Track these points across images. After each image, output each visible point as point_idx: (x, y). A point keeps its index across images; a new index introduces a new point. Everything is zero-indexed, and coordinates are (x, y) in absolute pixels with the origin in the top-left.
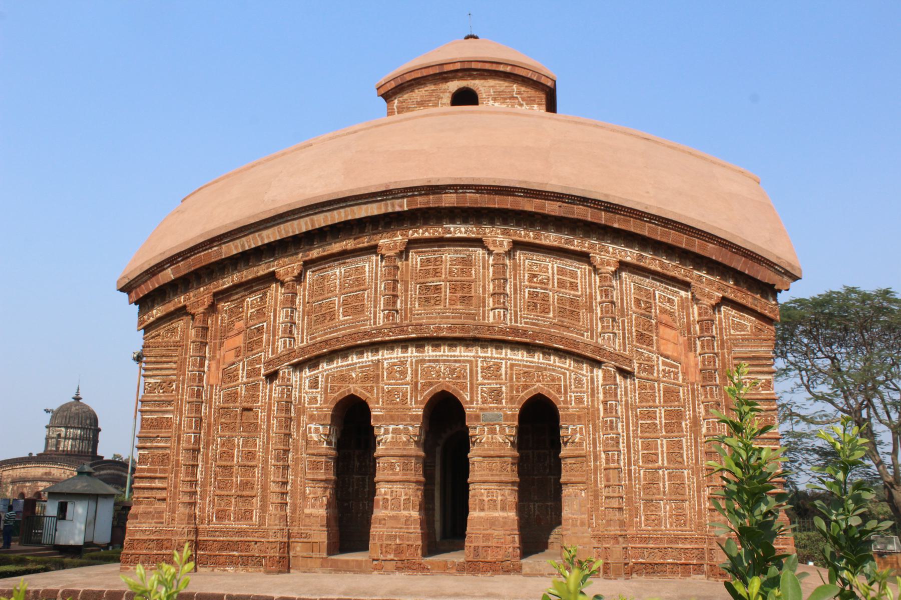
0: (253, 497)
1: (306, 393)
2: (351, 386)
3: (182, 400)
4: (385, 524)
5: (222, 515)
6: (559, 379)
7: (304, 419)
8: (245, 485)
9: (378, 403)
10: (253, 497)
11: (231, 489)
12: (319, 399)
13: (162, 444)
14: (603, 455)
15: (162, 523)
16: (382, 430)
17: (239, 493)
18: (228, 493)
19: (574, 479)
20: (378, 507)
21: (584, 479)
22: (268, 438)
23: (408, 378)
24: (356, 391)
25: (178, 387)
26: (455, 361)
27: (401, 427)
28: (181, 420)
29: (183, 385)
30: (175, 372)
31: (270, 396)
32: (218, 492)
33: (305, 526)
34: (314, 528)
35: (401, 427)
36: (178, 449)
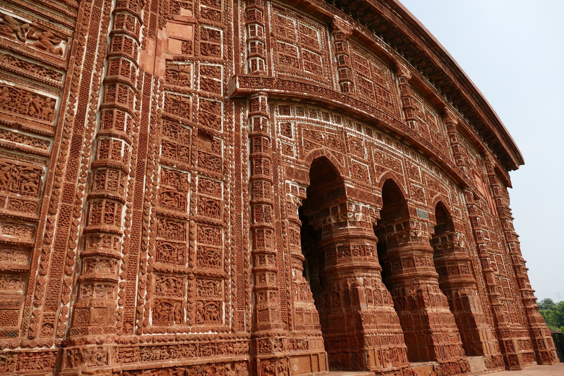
0: (219, 278)
1: (280, 138)
2: (323, 147)
3: (86, 76)
4: (375, 322)
5: (165, 312)
6: (446, 192)
7: (282, 171)
8: (206, 257)
9: (348, 175)
10: (219, 278)
11: (183, 264)
12: (294, 149)
13: (25, 145)
14: (479, 261)
15: (14, 334)
16: (354, 206)
17: (195, 269)
18: (178, 268)
19: (468, 280)
20: (363, 302)
21: (473, 279)
22: (238, 185)
23: (366, 158)
24: (328, 155)
25: (75, 50)
26: (393, 154)
27: (368, 206)
28: (82, 109)
29: (91, 48)
30: (70, 23)
31: (238, 126)
32: (158, 265)
33: (298, 328)
34: (309, 331)
35: (368, 206)
36: (73, 166)
